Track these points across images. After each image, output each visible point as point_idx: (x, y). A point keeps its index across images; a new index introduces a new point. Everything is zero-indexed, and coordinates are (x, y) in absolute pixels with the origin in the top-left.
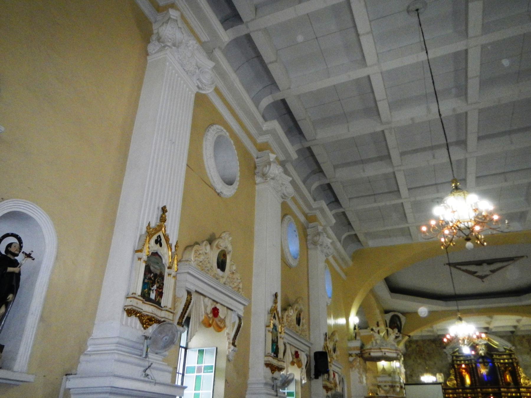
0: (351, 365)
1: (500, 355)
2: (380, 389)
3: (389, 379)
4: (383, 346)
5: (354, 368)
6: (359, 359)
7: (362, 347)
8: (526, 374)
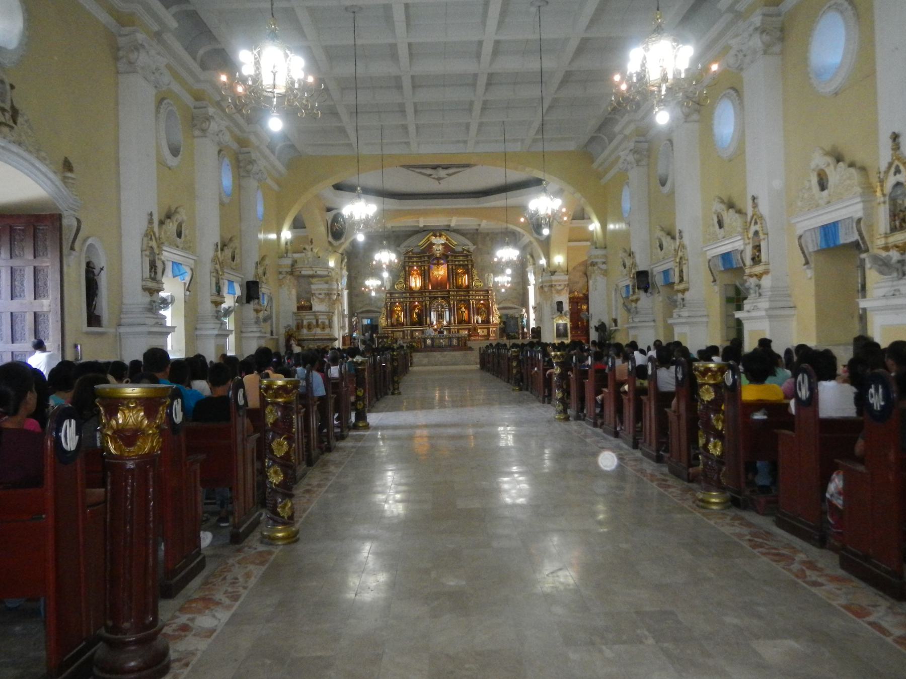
0: (280, 283)
1: (455, 257)
3: (326, 286)
5: (283, 286)
6: (289, 277)
7: (293, 265)
8: (479, 277)
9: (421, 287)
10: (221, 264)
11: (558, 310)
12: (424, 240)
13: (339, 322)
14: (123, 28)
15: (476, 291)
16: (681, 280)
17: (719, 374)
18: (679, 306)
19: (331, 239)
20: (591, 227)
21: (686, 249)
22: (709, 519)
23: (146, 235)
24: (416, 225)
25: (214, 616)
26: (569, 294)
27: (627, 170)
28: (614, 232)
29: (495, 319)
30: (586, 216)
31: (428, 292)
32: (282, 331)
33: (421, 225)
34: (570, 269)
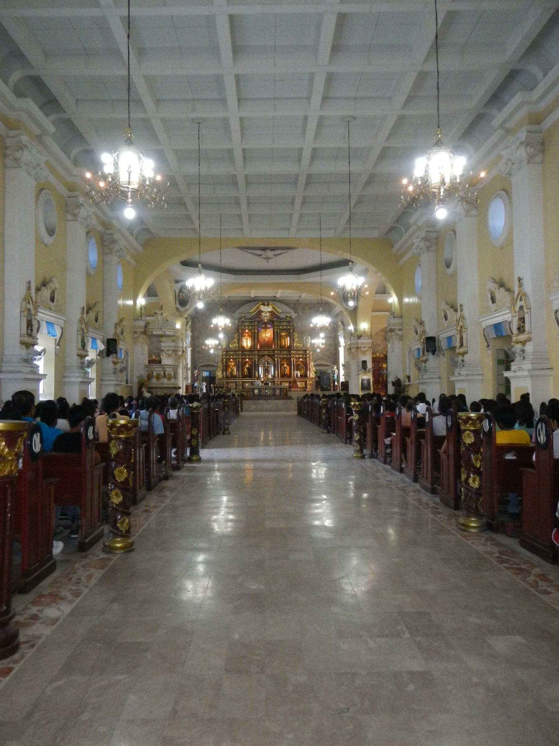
0: (135, 340)
1: (280, 322)
2: (163, 353)
3: (173, 344)
5: (137, 343)
6: (142, 336)
7: (146, 327)
9: (251, 346)
10: (86, 324)
11: (363, 368)
13: (183, 373)
14: (10, 131)
15: (296, 351)
16: (462, 345)
17: (478, 422)
18: (459, 366)
19: (178, 306)
20: (390, 300)
21: (466, 319)
22: (466, 539)
23: (25, 299)
25: (59, 609)
26: (372, 355)
27: (419, 254)
28: (408, 304)
29: (312, 374)
30: (386, 292)
31: (257, 350)
32: (136, 380)
33: (253, 295)
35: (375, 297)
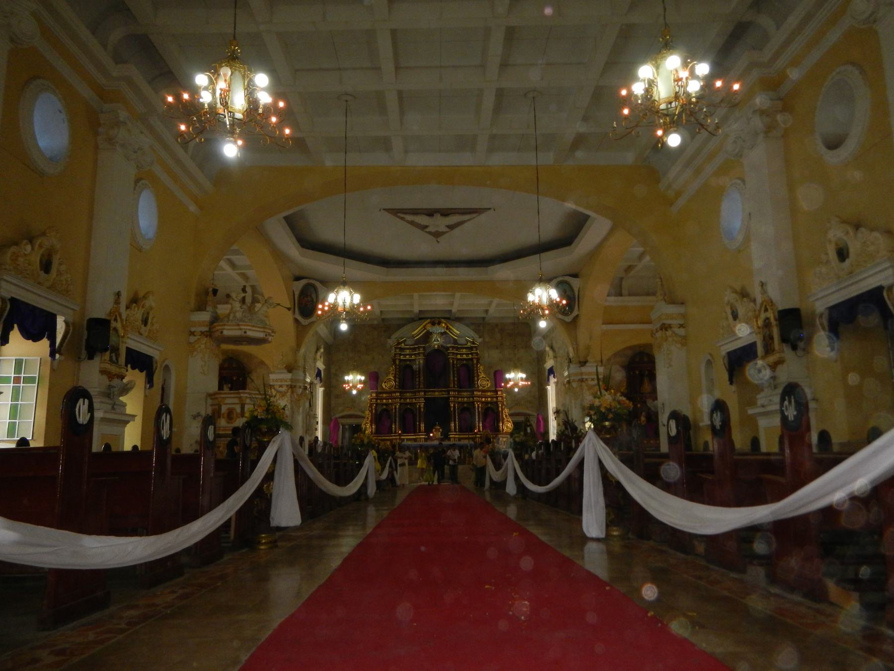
1: (457, 349)
2: (273, 390)
4: (244, 321)
5: (195, 353)
6: (205, 340)
8: (485, 374)
12: (419, 328)
24: (409, 309)
29: (508, 426)
31: (422, 391)
33: (416, 309)
34: (605, 359)
35: (606, 300)
